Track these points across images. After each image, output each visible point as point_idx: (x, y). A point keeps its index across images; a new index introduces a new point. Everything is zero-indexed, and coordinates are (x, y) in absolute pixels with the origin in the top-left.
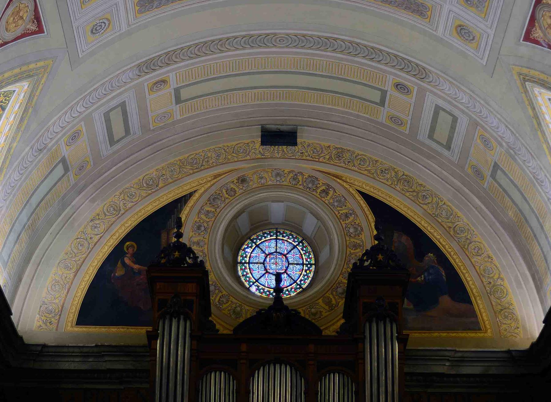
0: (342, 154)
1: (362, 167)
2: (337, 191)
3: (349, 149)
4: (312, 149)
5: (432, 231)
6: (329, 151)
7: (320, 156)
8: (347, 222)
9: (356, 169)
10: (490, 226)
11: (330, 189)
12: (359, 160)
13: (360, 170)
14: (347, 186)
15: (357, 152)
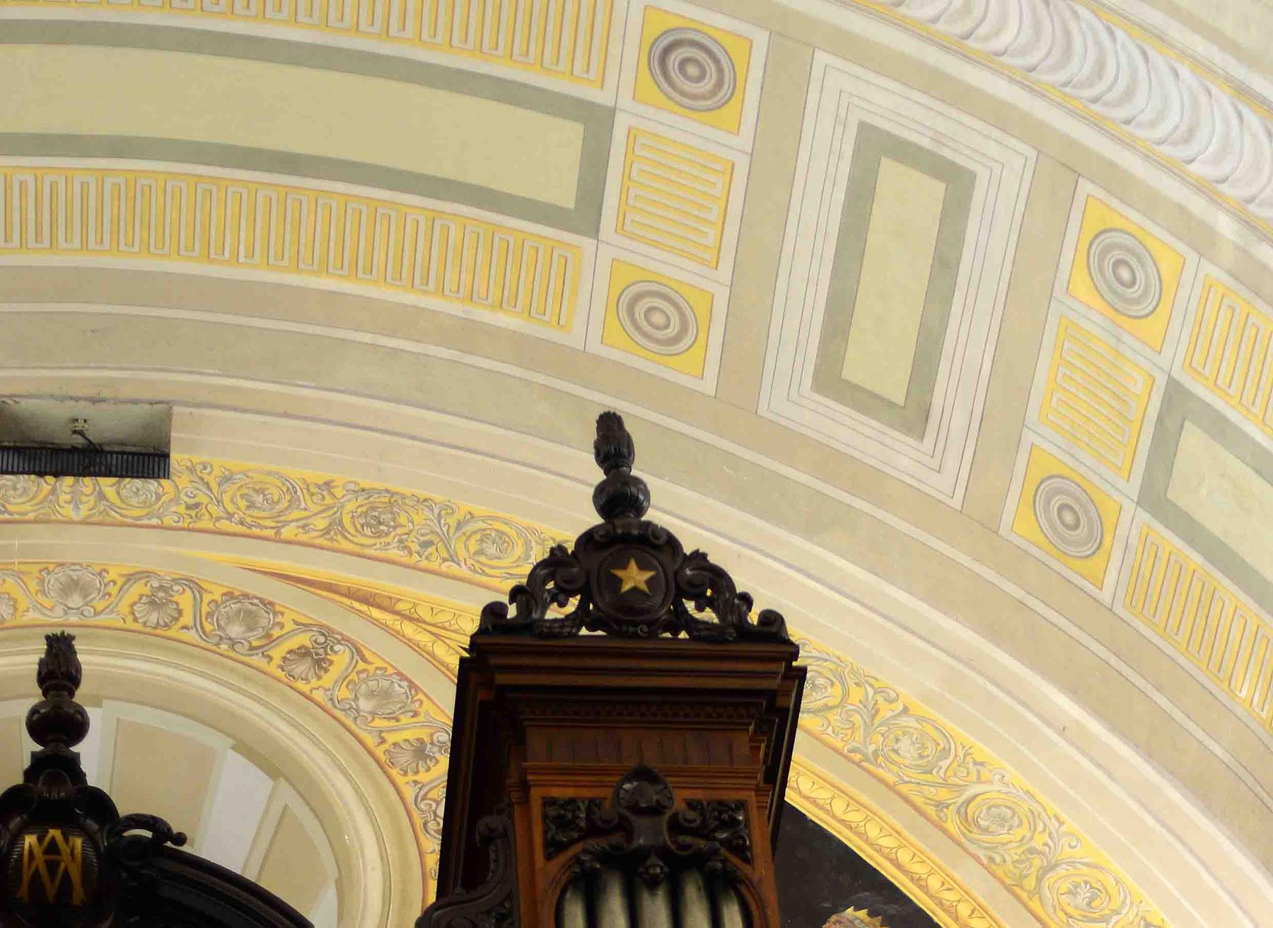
0: (392, 513)
1: (490, 563)
2: (367, 654)
3: (423, 494)
4: (245, 491)
5: (854, 817)
6: (329, 500)
7: (281, 519)
8: (423, 777)
9: (464, 571)
10: (1142, 805)
11: (336, 648)
12: (478, 536)
13: (484, 573)
14: (424, 638)
15: (466, 506)
